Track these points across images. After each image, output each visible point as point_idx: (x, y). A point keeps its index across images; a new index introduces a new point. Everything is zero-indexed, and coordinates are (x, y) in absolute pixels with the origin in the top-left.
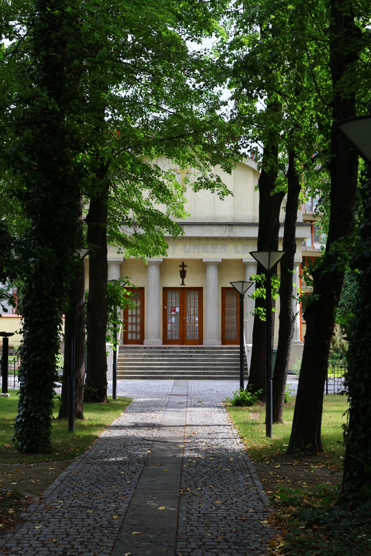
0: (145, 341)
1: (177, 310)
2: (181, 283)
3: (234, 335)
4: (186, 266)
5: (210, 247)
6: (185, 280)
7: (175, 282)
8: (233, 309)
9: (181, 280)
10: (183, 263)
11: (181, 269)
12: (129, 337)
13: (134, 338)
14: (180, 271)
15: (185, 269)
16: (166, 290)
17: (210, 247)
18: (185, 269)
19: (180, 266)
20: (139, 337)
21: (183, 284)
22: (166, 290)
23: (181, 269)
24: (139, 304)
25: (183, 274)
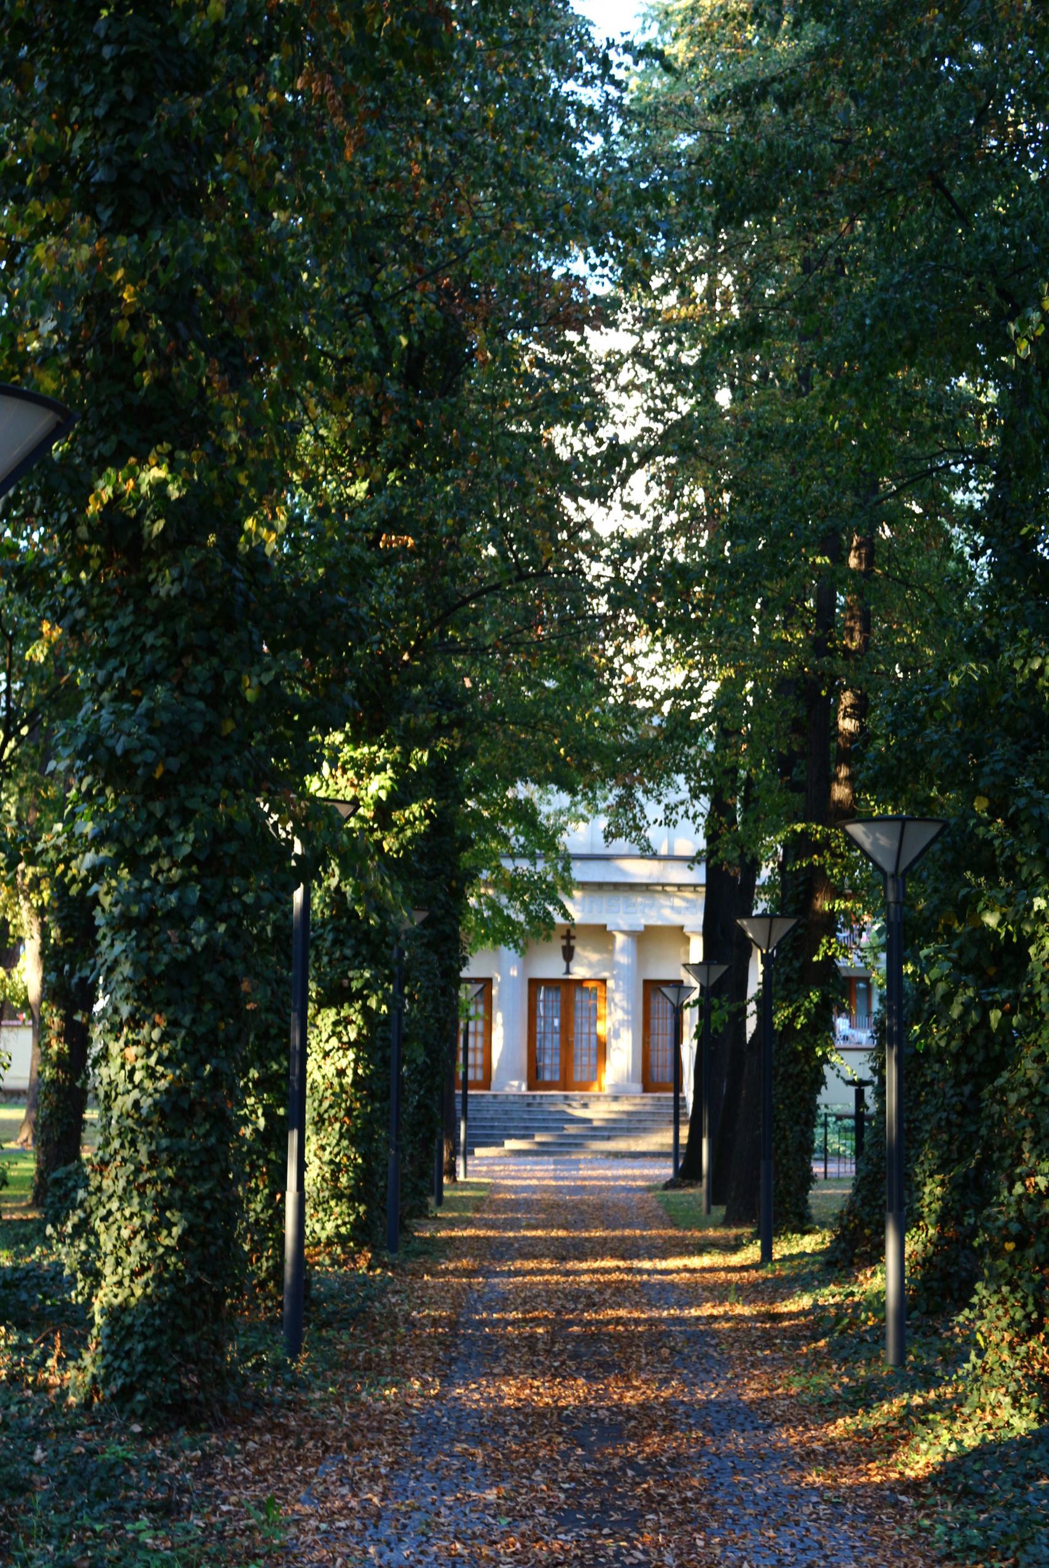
1: (556, 1022)
3: (664, 1073)
7: (551, 967)
8: (663, 1025)
16: (534, 984)
20: (480, 1076)
21: (568, 972)
22: (534, 984)
25: (568, 954)
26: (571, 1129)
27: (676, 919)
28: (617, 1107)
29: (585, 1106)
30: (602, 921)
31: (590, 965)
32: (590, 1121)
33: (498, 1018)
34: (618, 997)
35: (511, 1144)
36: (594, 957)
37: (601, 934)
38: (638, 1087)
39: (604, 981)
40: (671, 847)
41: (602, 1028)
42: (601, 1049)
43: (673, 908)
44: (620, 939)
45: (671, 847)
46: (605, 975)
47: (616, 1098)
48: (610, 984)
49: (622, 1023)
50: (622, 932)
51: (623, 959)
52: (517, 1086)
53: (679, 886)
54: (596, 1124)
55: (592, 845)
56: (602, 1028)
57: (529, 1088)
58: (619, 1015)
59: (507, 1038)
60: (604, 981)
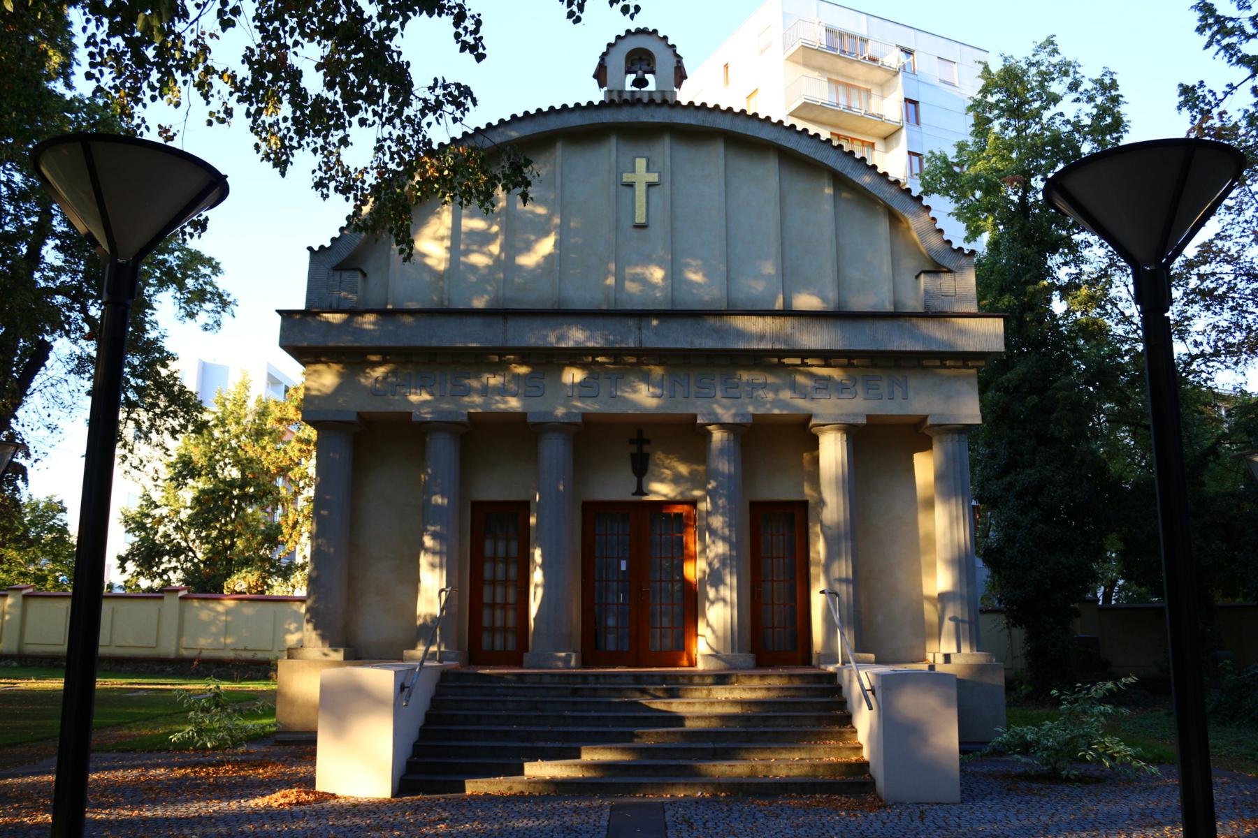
0: (526, 656)
2: (634, 489)
4: (648, 442)
5: (718, 379)
6: (644, 479)
7: (614, 487)
9: (635, 479)
10: (640, 432)
11: (634, 449)
12: (486, 645)
13: (498, 645)
14: (633, 455)
15: (646, 449)
17: (718, 379)
18: (646, 449)
19: (632, 442)
20: (511, 644)
21: (641, 491)
23: (634, 449)
24: (514, 548)
25: (641, 468)
26: (650, 737)
27: (803, 405)
28: (721, 693)
29: (673, 694)
30: (692, 411)
31: (677, 479)
32: (679, 720)
33: (537, 555)
34: (717, 522)
35: (539, 770)
36: (683, 469)
37: (686, 436)
38: (749, 659)
39: (693, 503)
40: (787, 301)
41: (694, 570)
42: (690, 605)
43: (794, 387)
44: (717, 435)
45: (787, 301)
46: (697, 493)
47: (721, 679)
48: (704, 506)
49: (723, 559)
50: (723, 426)
51: (724, 466)
52: (566, 660)
53: (805, 354)
54: (690, 725)
55: (673, 302)
56: (694, 570)
57: (584, 663)
58: (720, 548)
59: (547, 585)
60: (693, 503)
